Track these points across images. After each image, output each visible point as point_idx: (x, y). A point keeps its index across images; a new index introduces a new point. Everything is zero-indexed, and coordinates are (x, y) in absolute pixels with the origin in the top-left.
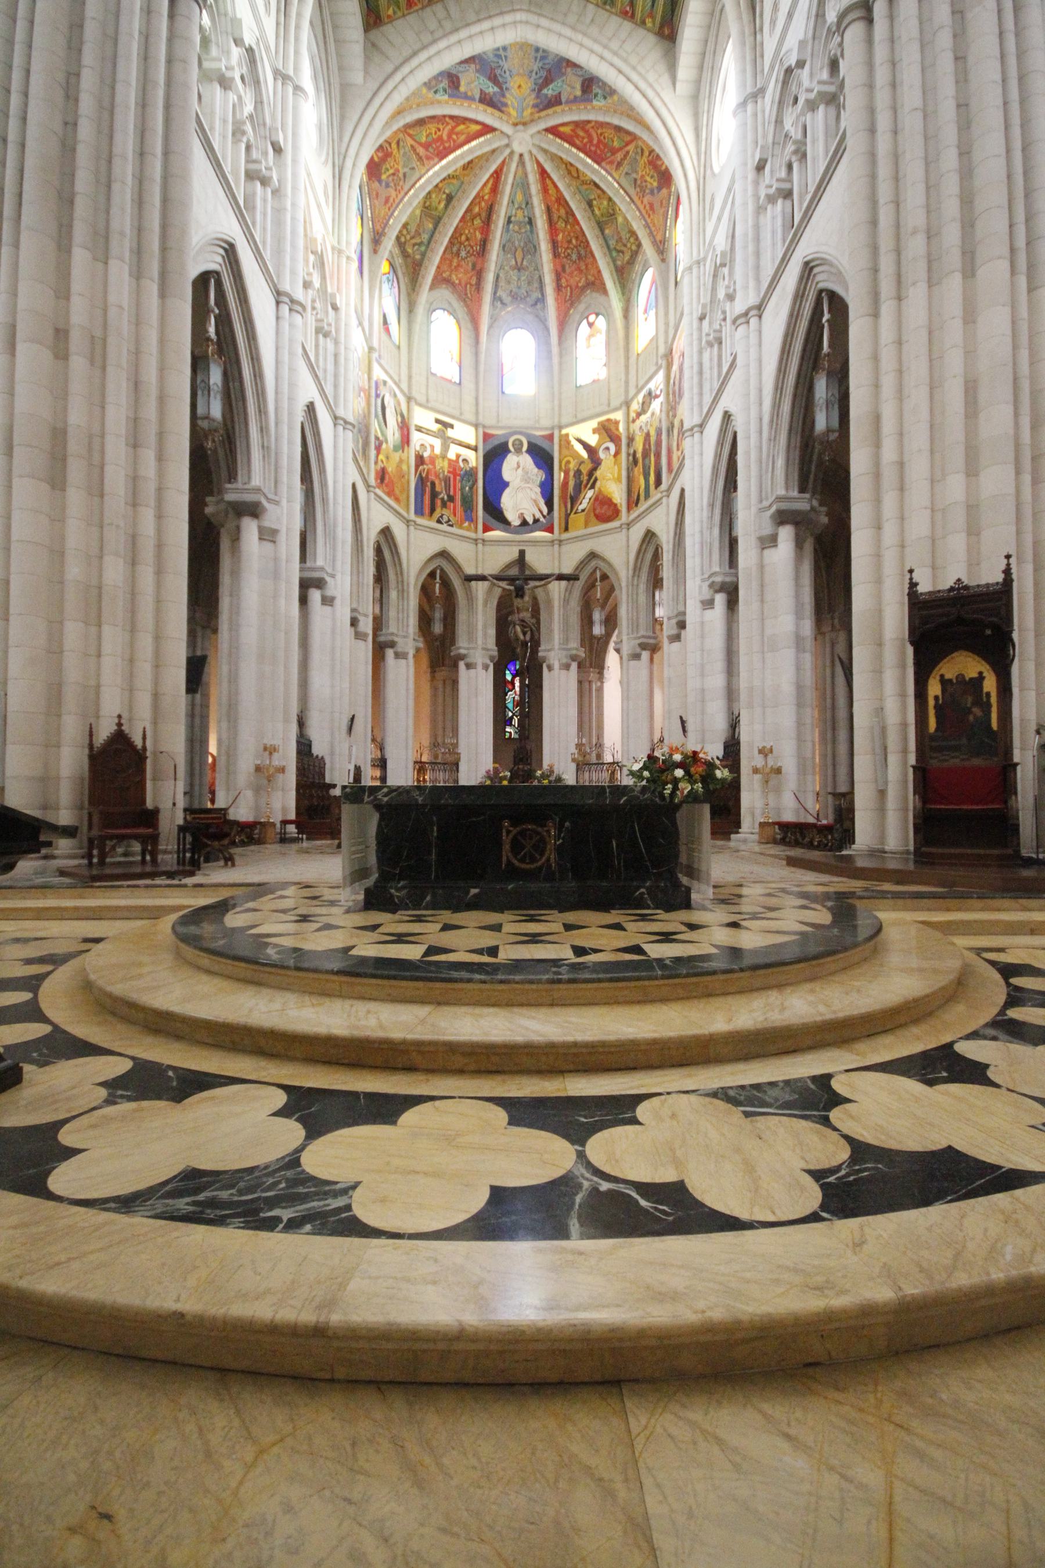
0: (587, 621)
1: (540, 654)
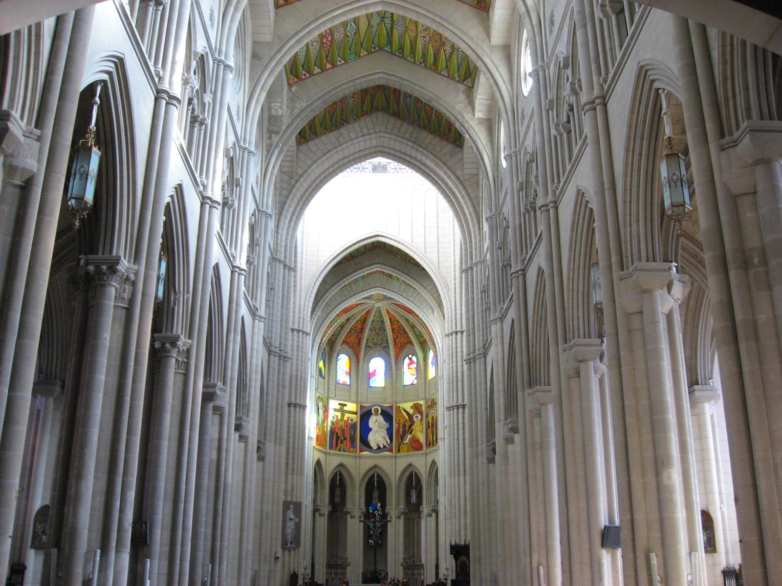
1: (386, 511)
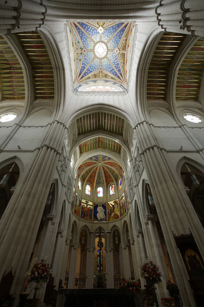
0: (114, 240)
